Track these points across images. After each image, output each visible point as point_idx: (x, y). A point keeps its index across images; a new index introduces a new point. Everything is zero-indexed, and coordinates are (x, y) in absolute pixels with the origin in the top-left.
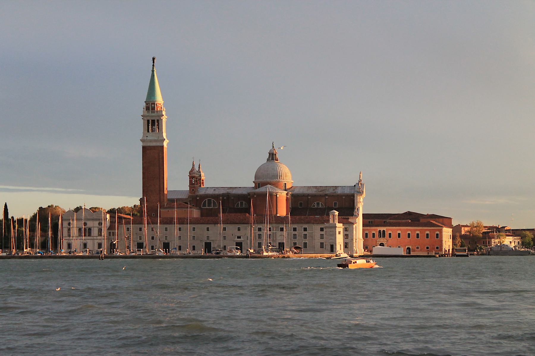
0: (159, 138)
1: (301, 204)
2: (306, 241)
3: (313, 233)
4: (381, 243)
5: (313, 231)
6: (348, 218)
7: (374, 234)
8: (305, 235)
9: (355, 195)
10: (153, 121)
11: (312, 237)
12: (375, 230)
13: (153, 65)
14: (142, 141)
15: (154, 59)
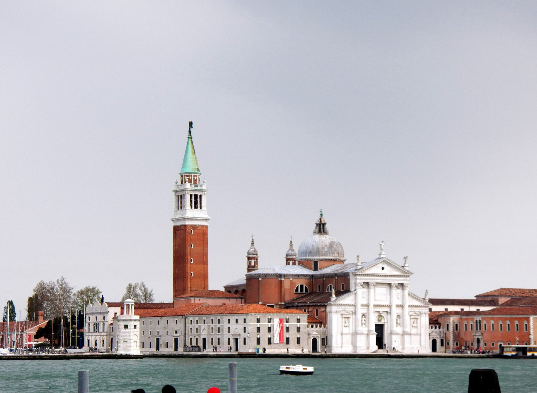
0: (183, 216)
1: (319, 286)
2: (219, 337)
3: (223, 325)
4: (477, 337)
5: (223, 323)
6: (326, 306)
7: (472, 324)
8: (219, 328)
9: (350, 274)
10: (181, 196)
11: (223, 331)
12: (472, 319)
13: (190, 132)
14: (173, 220)
15: (191, 124)
